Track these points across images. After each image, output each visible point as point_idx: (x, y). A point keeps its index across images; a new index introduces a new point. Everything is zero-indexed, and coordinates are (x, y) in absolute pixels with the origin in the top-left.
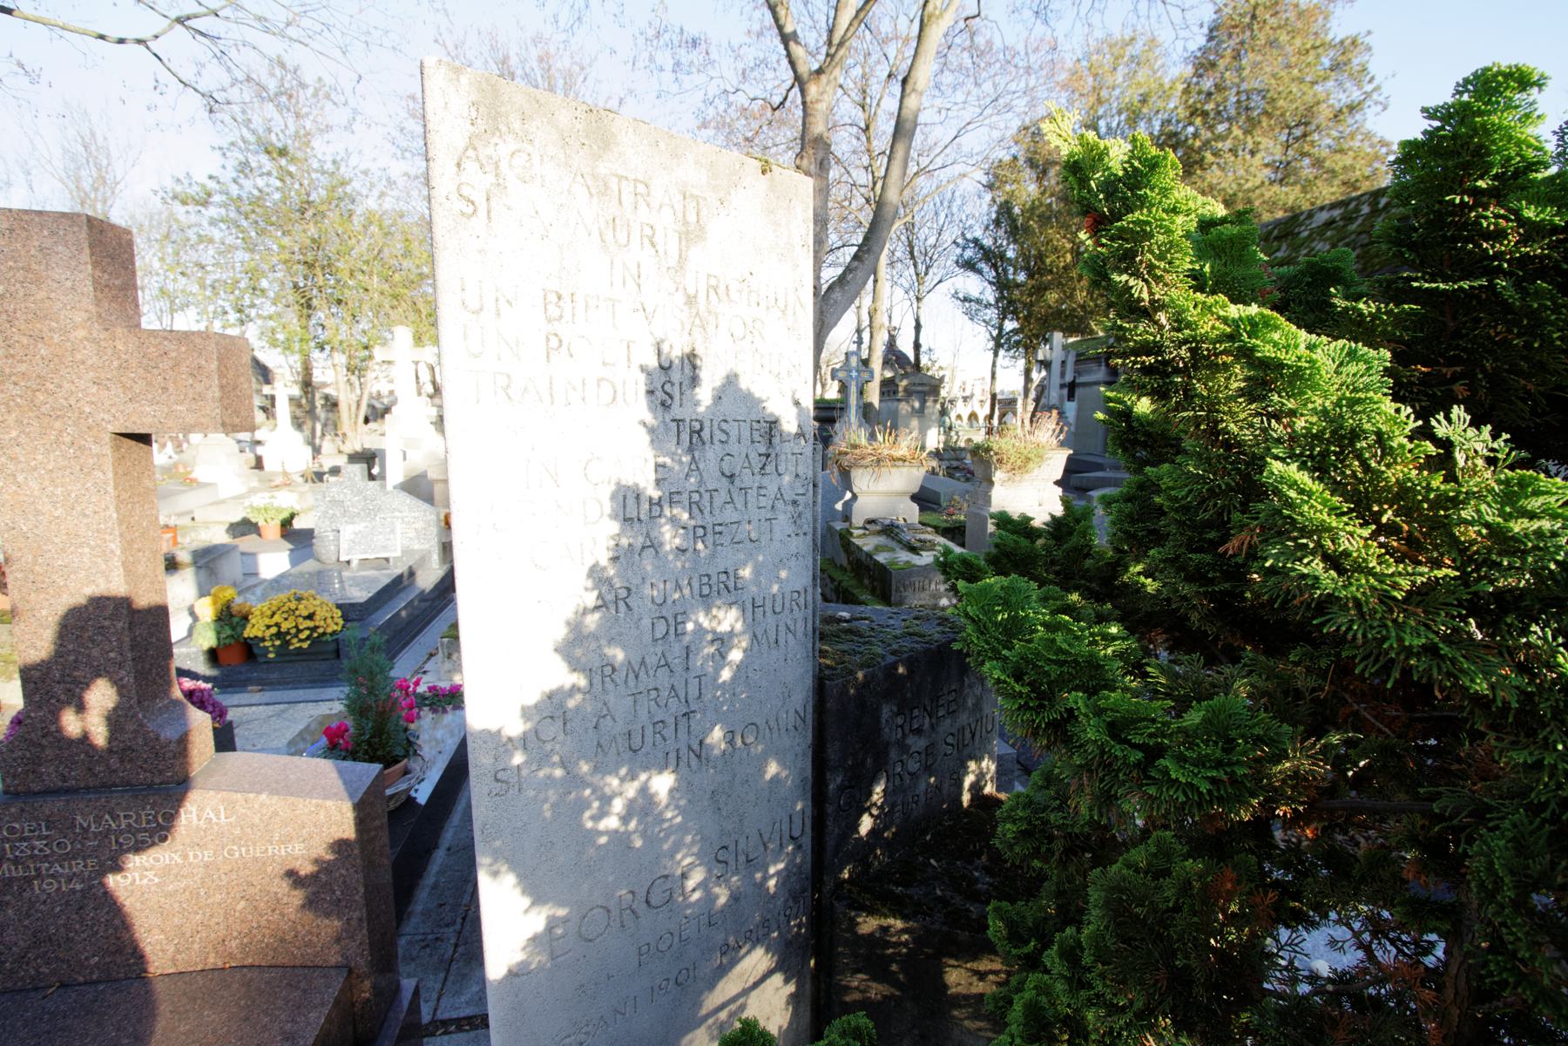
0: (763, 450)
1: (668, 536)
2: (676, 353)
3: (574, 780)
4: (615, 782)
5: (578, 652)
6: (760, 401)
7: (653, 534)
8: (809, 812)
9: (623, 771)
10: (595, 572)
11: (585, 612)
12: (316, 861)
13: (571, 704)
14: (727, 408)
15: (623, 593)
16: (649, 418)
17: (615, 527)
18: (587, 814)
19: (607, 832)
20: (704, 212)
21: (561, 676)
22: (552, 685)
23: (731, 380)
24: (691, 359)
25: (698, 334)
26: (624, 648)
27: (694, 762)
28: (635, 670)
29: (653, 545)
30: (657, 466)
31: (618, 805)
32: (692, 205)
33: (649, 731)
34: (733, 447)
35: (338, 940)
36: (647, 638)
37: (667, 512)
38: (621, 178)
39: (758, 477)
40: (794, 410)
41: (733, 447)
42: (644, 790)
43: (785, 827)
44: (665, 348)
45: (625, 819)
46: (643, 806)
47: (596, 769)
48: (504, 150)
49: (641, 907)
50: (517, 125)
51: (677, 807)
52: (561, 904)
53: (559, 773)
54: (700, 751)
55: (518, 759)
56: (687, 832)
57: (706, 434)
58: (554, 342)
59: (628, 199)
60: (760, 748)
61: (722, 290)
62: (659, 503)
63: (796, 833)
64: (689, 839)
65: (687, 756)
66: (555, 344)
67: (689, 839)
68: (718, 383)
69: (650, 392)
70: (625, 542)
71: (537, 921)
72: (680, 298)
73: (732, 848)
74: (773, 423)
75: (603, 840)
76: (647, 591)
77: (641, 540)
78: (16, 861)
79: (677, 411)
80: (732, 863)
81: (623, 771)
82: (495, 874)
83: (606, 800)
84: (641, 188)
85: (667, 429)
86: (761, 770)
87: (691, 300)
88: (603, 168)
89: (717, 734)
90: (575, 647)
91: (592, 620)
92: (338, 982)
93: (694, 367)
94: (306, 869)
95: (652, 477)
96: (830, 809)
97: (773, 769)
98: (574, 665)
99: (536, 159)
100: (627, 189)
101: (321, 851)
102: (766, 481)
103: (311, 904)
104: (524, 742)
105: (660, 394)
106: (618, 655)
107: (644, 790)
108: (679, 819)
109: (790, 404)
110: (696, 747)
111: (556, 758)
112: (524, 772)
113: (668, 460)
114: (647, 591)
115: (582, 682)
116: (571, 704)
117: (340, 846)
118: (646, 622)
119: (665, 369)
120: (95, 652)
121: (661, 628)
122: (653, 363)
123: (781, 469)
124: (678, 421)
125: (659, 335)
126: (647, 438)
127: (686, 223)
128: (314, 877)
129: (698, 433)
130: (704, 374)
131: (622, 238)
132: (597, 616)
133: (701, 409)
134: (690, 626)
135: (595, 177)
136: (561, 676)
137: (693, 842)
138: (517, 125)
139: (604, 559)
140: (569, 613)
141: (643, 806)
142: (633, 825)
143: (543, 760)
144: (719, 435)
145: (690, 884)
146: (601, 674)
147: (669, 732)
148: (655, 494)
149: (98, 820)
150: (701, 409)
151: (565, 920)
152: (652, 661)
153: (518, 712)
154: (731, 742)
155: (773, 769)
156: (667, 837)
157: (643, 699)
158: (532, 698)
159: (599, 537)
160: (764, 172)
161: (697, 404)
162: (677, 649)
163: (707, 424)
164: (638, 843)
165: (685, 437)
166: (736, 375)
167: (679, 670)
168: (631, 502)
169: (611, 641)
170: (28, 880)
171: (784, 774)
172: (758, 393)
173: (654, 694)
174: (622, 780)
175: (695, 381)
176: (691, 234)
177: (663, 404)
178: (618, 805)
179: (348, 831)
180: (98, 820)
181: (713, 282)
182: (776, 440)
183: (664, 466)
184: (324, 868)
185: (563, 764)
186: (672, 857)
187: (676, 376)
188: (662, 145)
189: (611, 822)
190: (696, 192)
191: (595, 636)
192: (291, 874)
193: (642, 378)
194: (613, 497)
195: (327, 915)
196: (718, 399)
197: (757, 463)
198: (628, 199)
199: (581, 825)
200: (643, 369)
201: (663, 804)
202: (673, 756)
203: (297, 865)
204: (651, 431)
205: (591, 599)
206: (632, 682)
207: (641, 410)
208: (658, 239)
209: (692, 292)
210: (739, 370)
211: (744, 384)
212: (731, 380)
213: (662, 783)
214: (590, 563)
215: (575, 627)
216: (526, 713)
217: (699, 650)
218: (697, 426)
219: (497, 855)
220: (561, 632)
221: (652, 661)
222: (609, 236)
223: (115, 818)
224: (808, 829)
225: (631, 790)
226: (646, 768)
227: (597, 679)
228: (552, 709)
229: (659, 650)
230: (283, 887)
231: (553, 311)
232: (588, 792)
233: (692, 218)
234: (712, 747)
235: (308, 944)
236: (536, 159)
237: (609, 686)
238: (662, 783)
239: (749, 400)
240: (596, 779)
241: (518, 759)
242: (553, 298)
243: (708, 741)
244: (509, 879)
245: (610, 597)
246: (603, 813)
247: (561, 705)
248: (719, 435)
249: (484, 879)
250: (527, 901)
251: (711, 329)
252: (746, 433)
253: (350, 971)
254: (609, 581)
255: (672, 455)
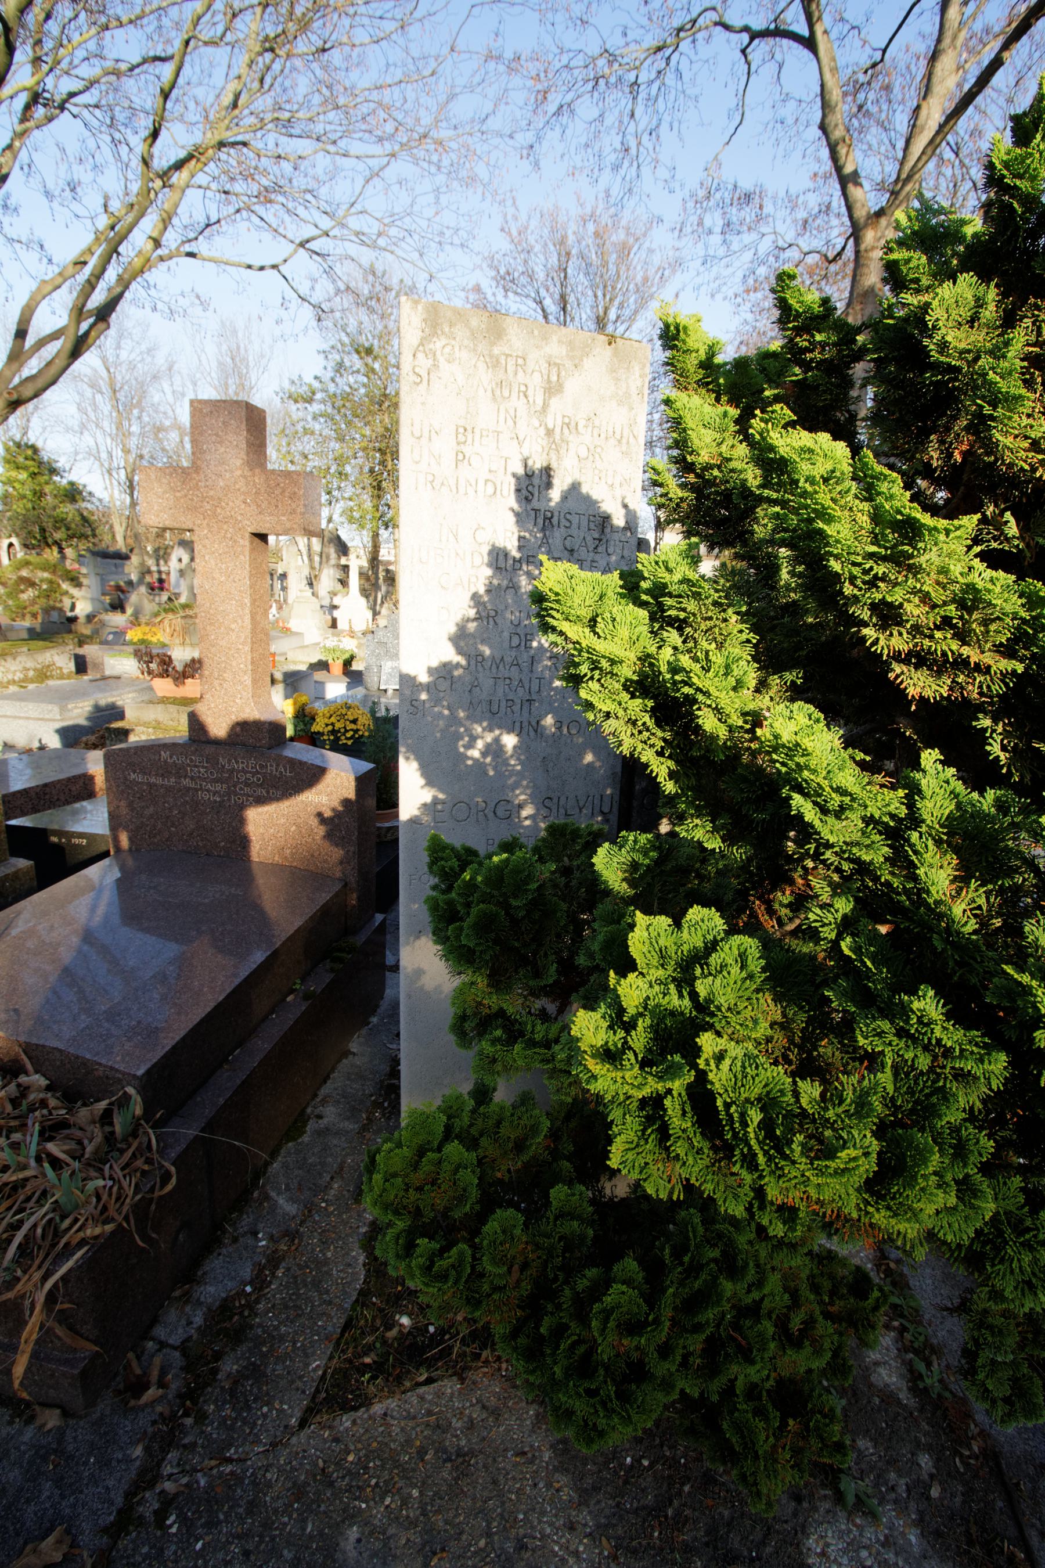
0: (597, 536)
1: (524, 583)
2: (538, 466)
3: (453, 720)
4: (479, 729)
5: (462, 644)
6: (596, 502)
7: (515, 580)
8: (617, 798)
9: (485, 724)
10: (475, 597)
11: (468, 620)
12: (333, 810)
13: (456, 673)
14: (571, 504)
15: (492, 613)
16: (516, 506)
17: (489, 572)
18: (461, 743)
19: (472, 758)
20: (563, 373)
21: (450, 654)
22: (446, 659)
23: (575, 487)
24: (547, 472)
25: (553, 456)
26: (490, 648)
27: (532, 733)
28: (498, 662)
29: (514, 587)
30: (520, 538)
31: (480, 744)
32: (555, 370)
33: (503, 704)
34: (574, 531)
35: (341, 863)
36: (506, 645)
37: (525, 567)
38: (507, 356)
39: (591, 554)
40: (623, 511)
41: (574, 531)
42: (497, 740)
43: (597, 802)
44: (530, 463)
45: (484, 754)
46: (495, 749)
47: (468, 718)
48: (439, 344)
49: (489, 812)
50: (447, 330)
51: (518, 759)
52: (441, 790)
53: (446, 712)
54: (537, 728)
55: (424, 696)
56: (524, 778)
57: (555, 521)
58: (460, 457)
59: (511, 368)
60: (581, 740)
61: (573, 424)
62: (520, 561)
63: (606, 810)
64: (525, 783)
65: (528, 730)
66: (460, 458)
67: (525, 783)
68: (565, 488)
69: (518, 491)
70: (495, 582)
71: (427, 795)
72: (542, 431)
73: (555, 800)
74: (606, 518)
75: (470, 762)
76: (508, 615)
77: (505, 582)
78: (192, 778)
79: (535, 504)
80: (555, 811)
81: (485, 724)
82: (407, 759)
83: (473, 739)
84: (520, 361)
85: (528, 515)
86: (581, 756)
87: (549, 433)
88: (496, 351)
89: (549, 720)
90: (460, 639)
91: (472, 626)
92: (338, 887)
93: (549, 476)
94: (328, 814)
95: (516, 544)
96: (635, 803)
97: (589, 758)
98: (460, 651)
99: (457, 349)
100: (511, 362)
101: (336, 804)
102: (597, 557)
103: (329, 836)
104: (427, 688)
105: (524, 492)
106: (487, 651)
107: (497, 740)
108: (519, 768)
109: (620, 506)
110: (534, 724)
111: (445, 703)
112: (427, 705)
113: (527, 535)
114: (508, 615)
115: (464, 662)
116: (456, 673)
117: (346, 802)
118: (506, 634)
119: (529, 475)
120: (234, 664)
121: (515, 641)
122: (521, 471)
123: (610, 551)
124: (536, 511)
125: (526, 454)
126: (513, 519)
127: (549, 381)
128: (331, 819)
129: (550, 519)
130: (556, 481)
131: (506, 394)
132: (475, 624)
133: (552, 504)
134: (535, 644)
135: (491, 356)
136: (450, 654)
137: (527, 787)
138: (447, 330)
139: (482, 590)
140: (458, 618)
141: (495, 749)
142: (488, 760)
143: (437, 702)
144: (564, 522)
145: (524, 813)
146: (474, 659)
147: (517, 708)
148: (518, 555)
149: (229, 761)
150: (552, 504)
151: (443, 802)
152: (508, 660)
153: (425, 669)
154: (559, 728)
155: (589, 758)
156: (510, 776)
157: (500, 682)
158: (435, 664)
159: (480, 577)
160: (610, 344)
161: (550, 500)
162: (525, 657)
163: (556, 514)
164: (491, 773)
165: (540, 521)
166: (579, 484)
167: (526, 670)
168: (501, 557)
169: (483, 642)
170: (197, 790)
171: (598, 764)
172: (595, 496)
173: (508, 681)
174: (484, 729)
175: (549, 485)
176: (553, 389)
177: (526, 498)
178: (480, 744)
179: (351, 794)
180: (229, 761)
181: (567, 420)
182: (608, 530)
183: (524, 538)
184: (337, 814)
185: (449, 708)
186: (513, 790)
187: (536, 481)
188: (536, 332)
189: (475, 753)
190: (558, 361)
191: (472, 636)
192: (320, 815)
193: (513, 481)
194: (490, 553)
195: (337, 845)
196: (565, 497)
197: (591, 545)
198: (511, 368)
199: (457, 749)
200: (514, 475)
201: (510, 753)
202: (518, 725)
203: (323, 809)
204: (517, 515)
205: (472, 613)
206: (494, 670)
207: (511, 501)
208: (530, 393)
209: (550, 426)
210: (582, 480)
211: (584, 489)
212: (575, 487)
213: (510, 741)
214: (473, 590)
215: (462, 628)
216: (430, 671)
217: (540, 661)
218: (549, 515)
219: (411, 749)
220: (453, 629)
221: (508, 660)
222: (498, 392)
223: (237, 762)
224: (615, 810)
225: (489, 738)
226: (500, 727)
227: (473, 662)
228: (443, 672)
229: (513, 654)
230: (314, 822)
231: (461, 438)
232: (462, 730)
233: (554, 378)
234: (544, 728)
235: (326, 861)
236: (457, 349)
237: (480, 669)
238: (510, 741)
239: (588, 500)
240: (468, 723)
241: (424, 696)
242: (461, 430)
243: (543, 723)
244: (415, 765)
245: (484, 614)
246: (470, 746)
247: (450, 672)
248: (564, 522)
249: (402, 761)
250: (422, 782)
251: (563, 451)
252: (584, 523)
253: (346, 885)
254: (484, 604)
255: (531, 532)
